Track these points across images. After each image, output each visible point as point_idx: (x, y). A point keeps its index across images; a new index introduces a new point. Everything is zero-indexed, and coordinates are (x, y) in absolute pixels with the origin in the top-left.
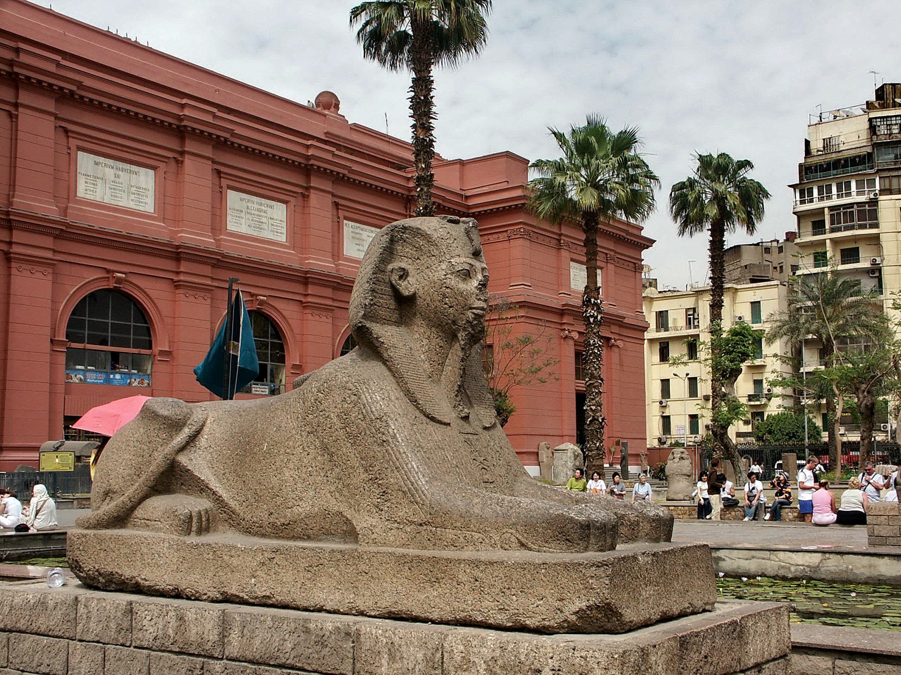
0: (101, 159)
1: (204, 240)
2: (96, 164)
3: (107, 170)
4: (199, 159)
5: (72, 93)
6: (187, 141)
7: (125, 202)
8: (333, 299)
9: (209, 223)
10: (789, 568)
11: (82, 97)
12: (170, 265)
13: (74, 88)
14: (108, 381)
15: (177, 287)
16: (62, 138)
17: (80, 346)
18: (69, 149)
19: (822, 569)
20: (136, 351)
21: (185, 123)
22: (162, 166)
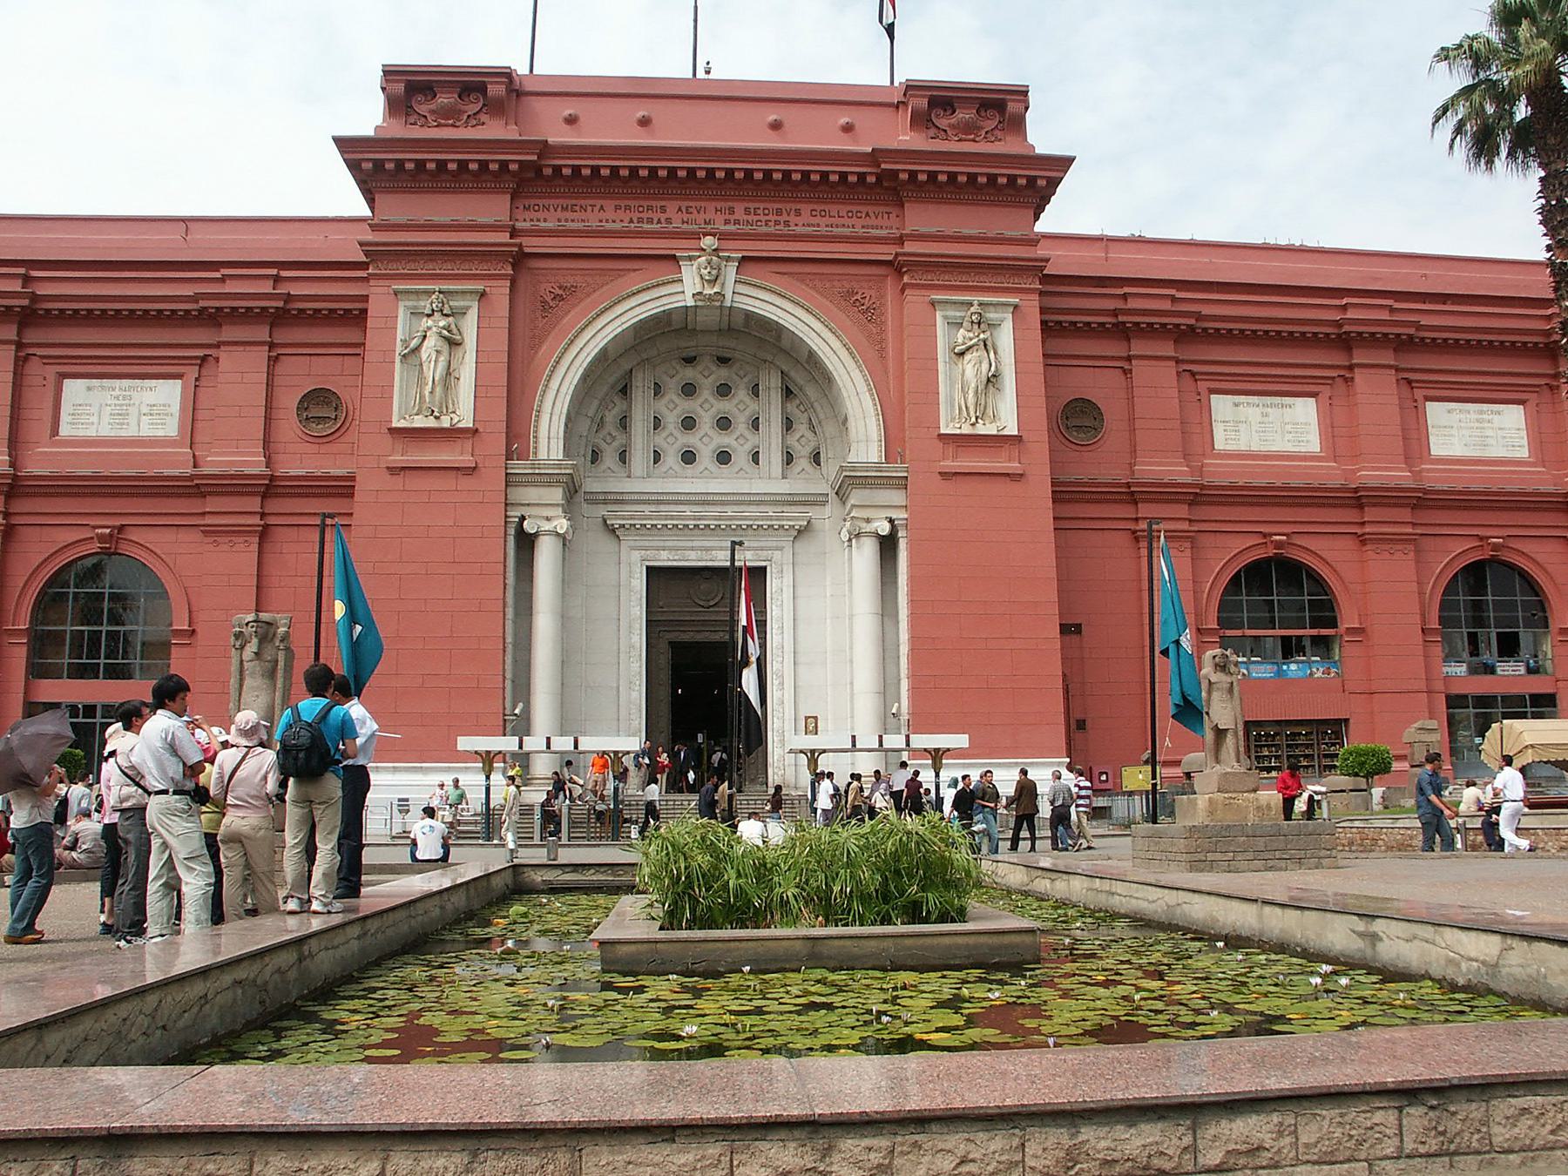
0: (1242, 398)
1: (1397, 475)
3: (1251, 410)
4: (1372, 371)
5: (1192, 328)
6: (1355, 352)
7: (1281, 443)
8: (1414, 524)
9: (1401, 451)
10: (1458, 965)
11: (1205, 330)
12: (1350, 515)
14: (1280, 673)
15: (1363, 542)
17: (1238, 633)
19: (1504, 971)
20: (1314, 632)
21: (1346, 328)
22: (1326, 391)
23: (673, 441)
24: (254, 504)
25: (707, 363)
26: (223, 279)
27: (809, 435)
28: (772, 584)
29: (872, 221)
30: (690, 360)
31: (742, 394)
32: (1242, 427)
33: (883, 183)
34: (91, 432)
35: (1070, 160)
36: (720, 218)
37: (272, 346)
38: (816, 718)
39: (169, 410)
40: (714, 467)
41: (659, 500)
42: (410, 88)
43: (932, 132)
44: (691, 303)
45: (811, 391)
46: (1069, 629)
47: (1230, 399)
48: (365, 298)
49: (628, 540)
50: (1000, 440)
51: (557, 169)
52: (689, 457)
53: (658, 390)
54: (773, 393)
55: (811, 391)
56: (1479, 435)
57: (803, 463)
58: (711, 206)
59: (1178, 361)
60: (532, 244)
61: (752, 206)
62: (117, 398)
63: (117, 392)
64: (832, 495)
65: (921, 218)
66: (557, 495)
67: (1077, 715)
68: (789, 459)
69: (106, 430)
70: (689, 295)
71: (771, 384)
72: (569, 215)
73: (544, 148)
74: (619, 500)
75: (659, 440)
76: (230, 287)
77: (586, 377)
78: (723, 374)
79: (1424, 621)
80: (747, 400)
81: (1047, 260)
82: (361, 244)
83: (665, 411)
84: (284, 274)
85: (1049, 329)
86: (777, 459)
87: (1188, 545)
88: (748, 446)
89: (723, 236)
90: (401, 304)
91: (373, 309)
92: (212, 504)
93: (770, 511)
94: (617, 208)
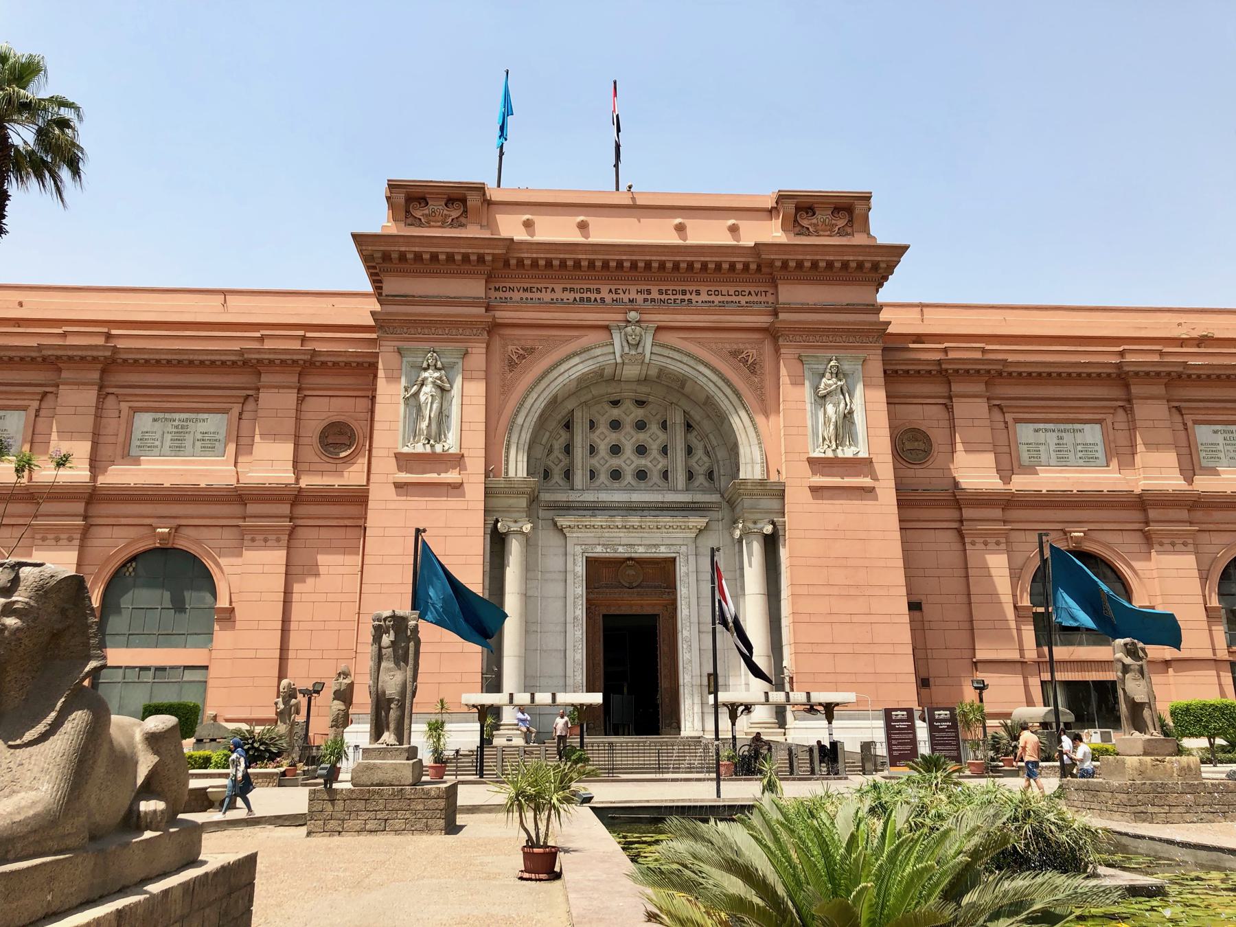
0: (1041, 426)
2: (1036, 431)
3: (1048, 434)
5: (1000, 374)
11: (1010, 374)
13: (1000, 367)
16: (997, 416)
18: (1006, 423)
23: (605, 462)
24: (285, 509)
25: (628, 404)
26: (262, 339)
27: (706, 459)
29: (753, 298)
30: (615, 403)
32: (1042, 448)
33: (761, 269)
35: (906, 248)
36: (640, 298)
37: (299, 390)
39: (217, 437)
40: (633, 482)
41: (594, 508)
42: (409, 198)
43: (797, 229)
44: (619, 360)
46: (914, 606)
47: (1032, 426)
51: (520, 262)
52: (616, 475)
53: (592, 425)
54: (678, 428)
55: (707, 425)
57: (701, 480)
58: (633, 289)
60: (503, 315)
61: (664, 288)
62: (177, 427)
63: (176, 423)
64: (724, 504)
65: (790, 293)
66: (523, 502)
67: (923, 675)
68: (690, 476)
70: (618, 355)
72: (529, 295)
75: (594, 461)
76: (268, 345)
77: (541, 416)
78: (639, 413)
79: (1205, 604)
80: (659, 433)
81: (889, 323)
82: (373, 313)
83: (598, 440)
86: (680, 478)
87: (1003, 540)
88: (660, 466)
90: (405, 360)
92: (252, 508)
94: (564, 290)
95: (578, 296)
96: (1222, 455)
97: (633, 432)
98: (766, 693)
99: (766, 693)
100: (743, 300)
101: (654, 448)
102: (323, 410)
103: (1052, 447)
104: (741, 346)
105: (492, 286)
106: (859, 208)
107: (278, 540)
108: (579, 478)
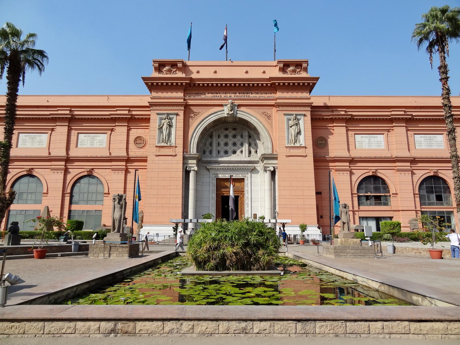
2: (362, 137)
7: (374, 147)
23: (222, 148)
24: (124, 163)
25: (230, 130)
27: (255, 147)
28: (246, 181)
29: (269, 95)
30: (226, 129)
31: (239, 137)
32: (363, 143)
34: (85, 146)
37: (128, 126)
38: (256, 214)
42: (160, 66)
44: (226, 116)
45: (255, 136)
46: (318, 193)
48: (149, 115)
49: (212, 172)
50: (300, 147)
51: (194, 84)
55: (255, 136)
56: (432, 144)
59: (346, 127)
66: (195, 161)
68: (250, 152)
69: (89, 146)
71: (246, 134)
73: (191, 79)
74: (210, 162)
75: (219, 148)
84: (131, 109)
85: (313, 120)
89: (234, 100)
91: (152, 117)
93: (245, 165)
94: (208, 94)
95: (213, 95)
96: (423, 145)
97: (232, 138)
98: (270, 220)
99: (270, 220)
100: (266, 95)
101: (238, 144)
102: (135, 133)
103: (367, 142)
104: (265, 111)
105: (186, 92)
106: (304, 65)
107: (122, 173)
108: (214, 153)
